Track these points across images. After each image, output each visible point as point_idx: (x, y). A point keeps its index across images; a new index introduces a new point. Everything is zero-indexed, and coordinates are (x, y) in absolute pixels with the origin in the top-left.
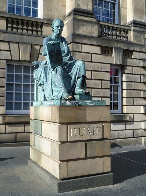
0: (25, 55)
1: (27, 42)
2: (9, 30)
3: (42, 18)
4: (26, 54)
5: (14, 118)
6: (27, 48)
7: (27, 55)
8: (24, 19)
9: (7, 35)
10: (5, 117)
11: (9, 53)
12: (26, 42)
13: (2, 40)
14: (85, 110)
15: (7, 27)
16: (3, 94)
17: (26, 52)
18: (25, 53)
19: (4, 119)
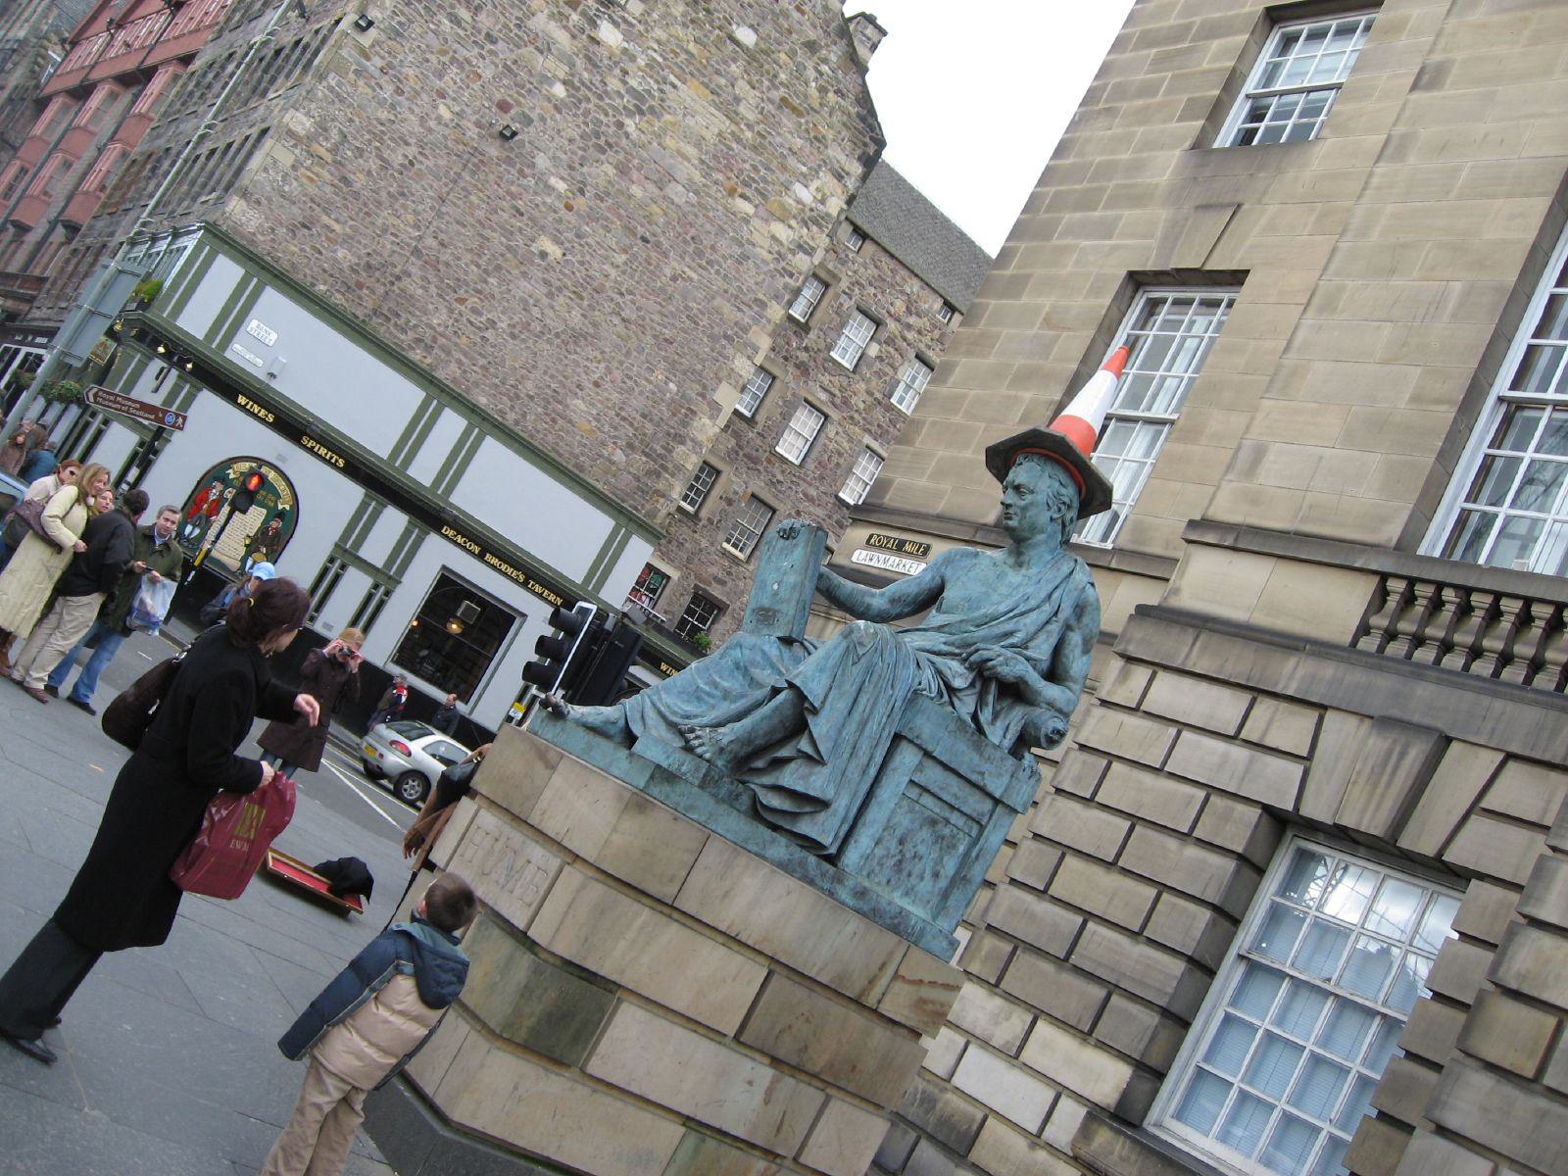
0: (1371, 795)
1: (1426, 721)
2: (1369, 644)
3: (1550, 570)
4: (1379, 791)
5: (1133, 1157)
6: (1403, 755)
7: (1383, 796)
8: (1471, 583)
9: (1328, 670)
10: (1095, 1126)
11: (1297, 770)
12: (1416, 718)
13: (1290, 692)
14: (552, 767)
15: (1364, 629)
16: (1159, 990)
17: (1385, 778)
18: (1375, 787)
19: (1085, 1131)
